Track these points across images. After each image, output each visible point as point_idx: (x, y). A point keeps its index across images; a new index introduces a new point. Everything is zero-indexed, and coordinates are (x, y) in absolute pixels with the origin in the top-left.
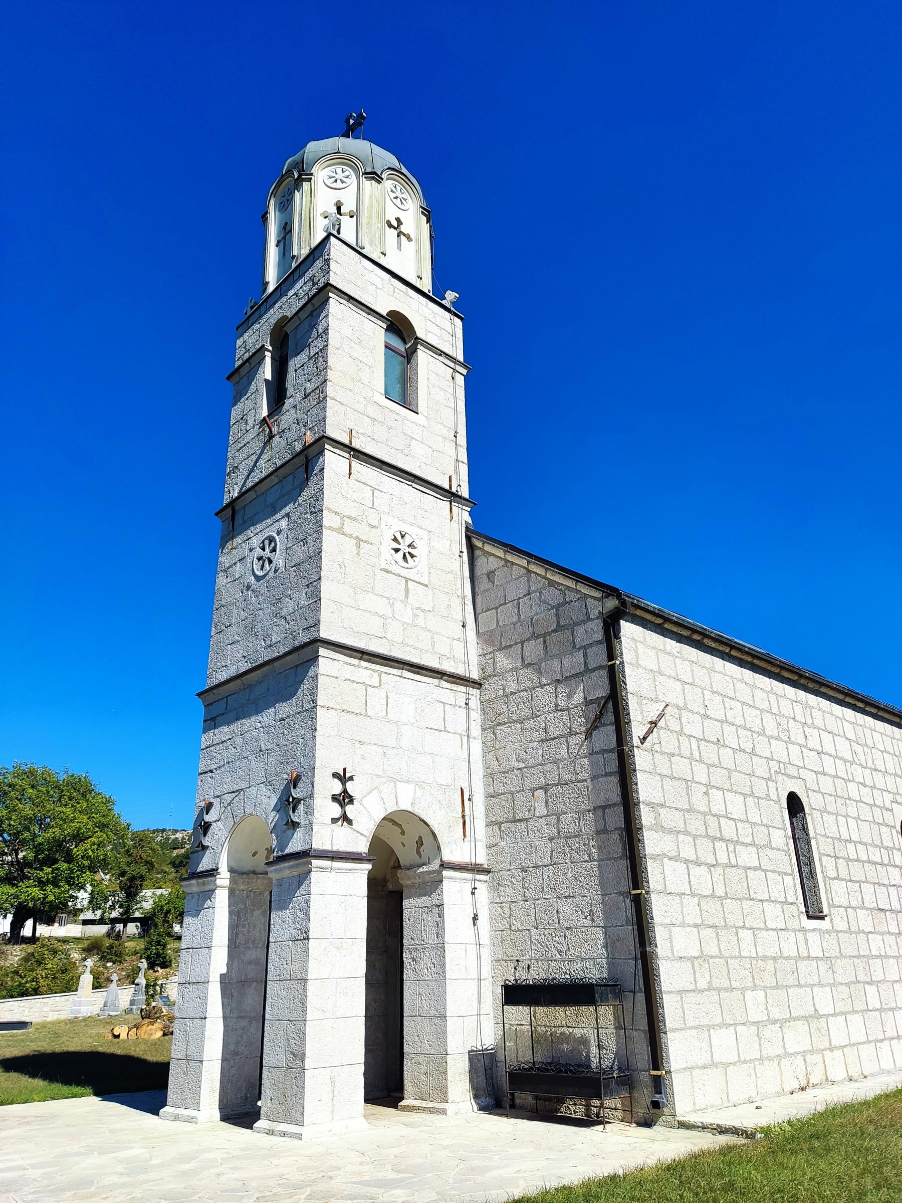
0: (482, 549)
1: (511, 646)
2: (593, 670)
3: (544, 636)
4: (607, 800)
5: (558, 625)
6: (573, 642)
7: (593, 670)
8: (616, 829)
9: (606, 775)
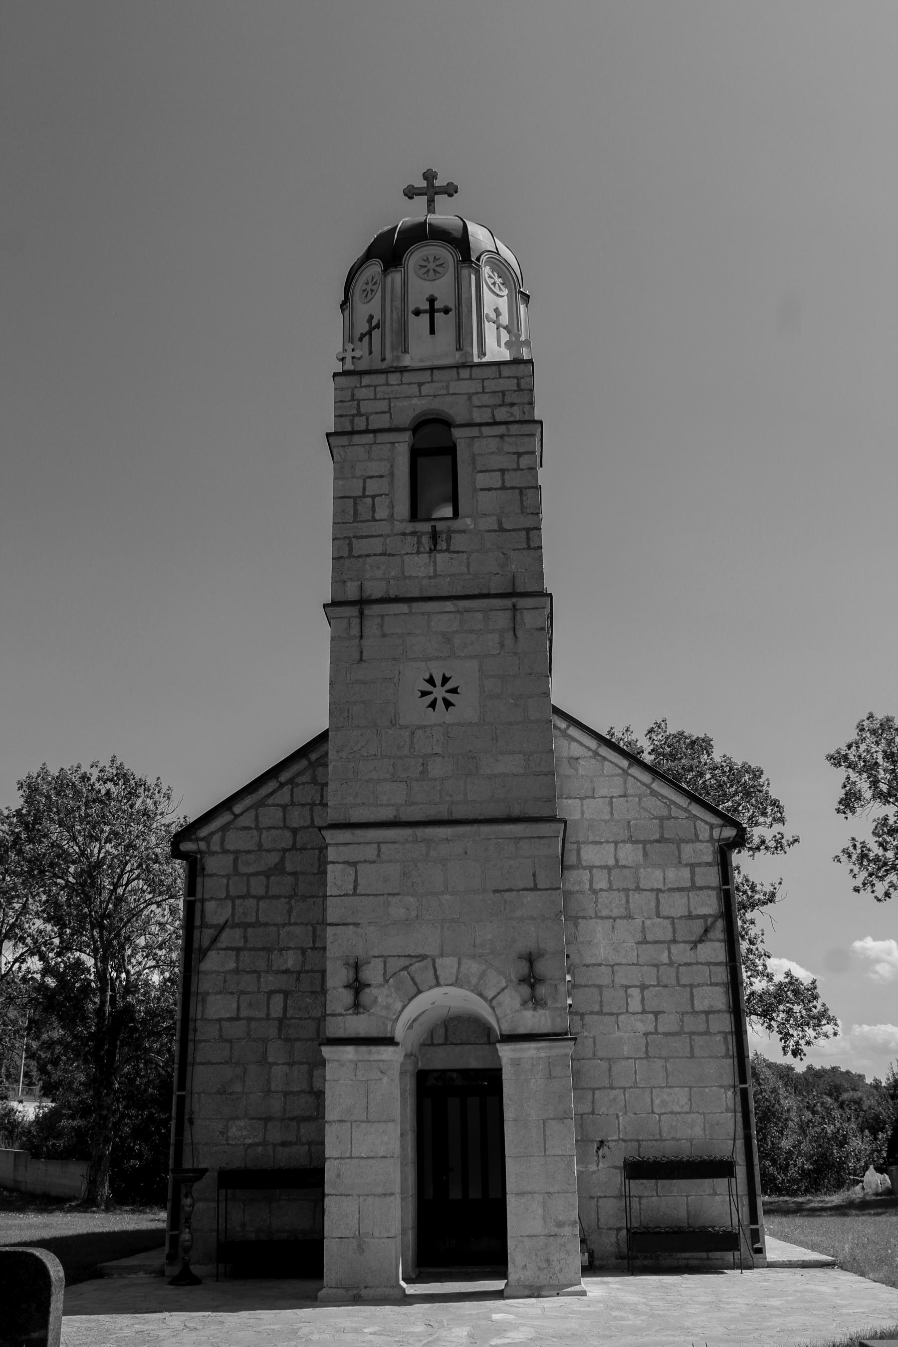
0: (564, 733)
1: (601, 843)
2: (701, 888)
3: (644, 843)
4: (712, 1006)
5: (662, 836)
6: (679, 857)
7: (701, 888)
8: (719, 1032)
9: (712, 984)
